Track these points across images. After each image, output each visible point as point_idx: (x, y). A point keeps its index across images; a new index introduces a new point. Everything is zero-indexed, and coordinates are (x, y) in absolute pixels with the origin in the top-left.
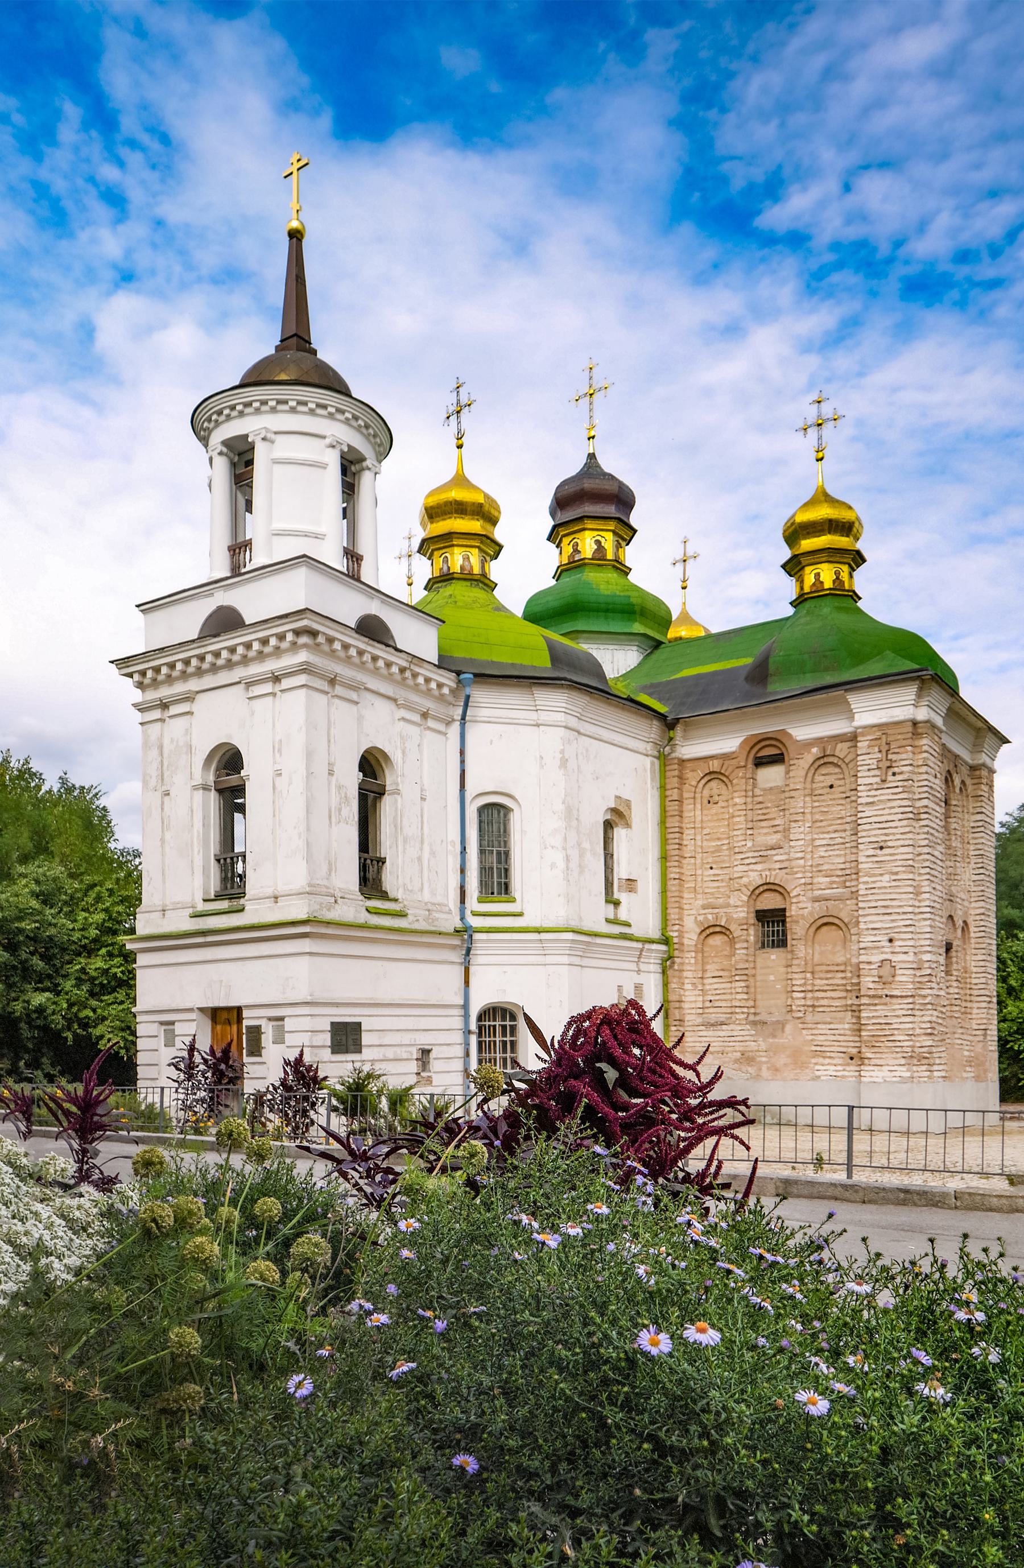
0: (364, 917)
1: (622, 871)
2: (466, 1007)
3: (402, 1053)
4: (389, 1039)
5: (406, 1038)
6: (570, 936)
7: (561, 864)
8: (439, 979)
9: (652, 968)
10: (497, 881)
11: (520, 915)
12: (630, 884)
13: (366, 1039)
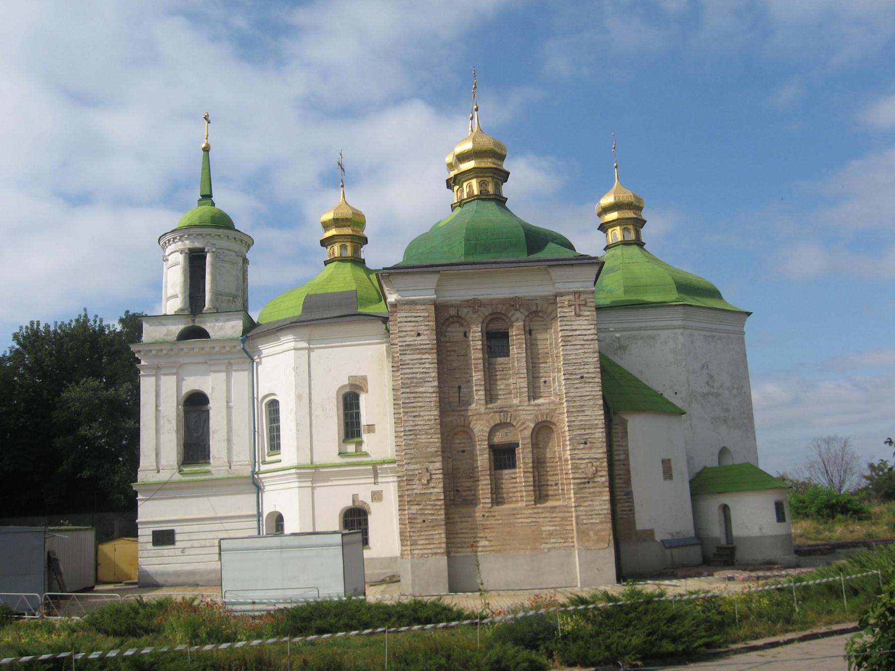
0: (178, 477)
1: (364, 420)
2: (259, 515)
3: (208, 543)
4: (203, 536)
5: (210, 536)
6: (294, 471)
7: (294, 430)
8: (244, 503)
9: (391, 479)
10: (275, 445)
11: (280, 461)
12: (371, 428)
13: (177, 537)
